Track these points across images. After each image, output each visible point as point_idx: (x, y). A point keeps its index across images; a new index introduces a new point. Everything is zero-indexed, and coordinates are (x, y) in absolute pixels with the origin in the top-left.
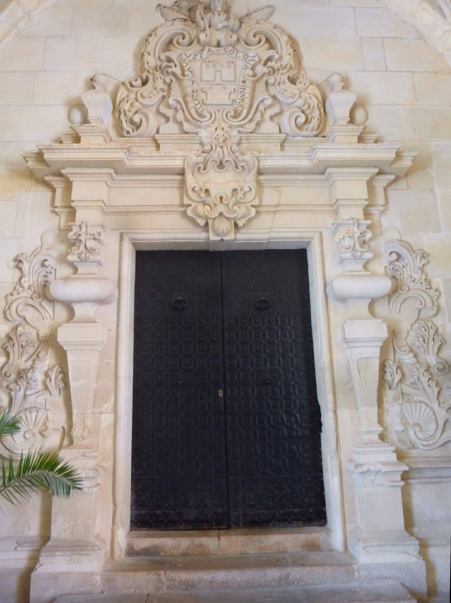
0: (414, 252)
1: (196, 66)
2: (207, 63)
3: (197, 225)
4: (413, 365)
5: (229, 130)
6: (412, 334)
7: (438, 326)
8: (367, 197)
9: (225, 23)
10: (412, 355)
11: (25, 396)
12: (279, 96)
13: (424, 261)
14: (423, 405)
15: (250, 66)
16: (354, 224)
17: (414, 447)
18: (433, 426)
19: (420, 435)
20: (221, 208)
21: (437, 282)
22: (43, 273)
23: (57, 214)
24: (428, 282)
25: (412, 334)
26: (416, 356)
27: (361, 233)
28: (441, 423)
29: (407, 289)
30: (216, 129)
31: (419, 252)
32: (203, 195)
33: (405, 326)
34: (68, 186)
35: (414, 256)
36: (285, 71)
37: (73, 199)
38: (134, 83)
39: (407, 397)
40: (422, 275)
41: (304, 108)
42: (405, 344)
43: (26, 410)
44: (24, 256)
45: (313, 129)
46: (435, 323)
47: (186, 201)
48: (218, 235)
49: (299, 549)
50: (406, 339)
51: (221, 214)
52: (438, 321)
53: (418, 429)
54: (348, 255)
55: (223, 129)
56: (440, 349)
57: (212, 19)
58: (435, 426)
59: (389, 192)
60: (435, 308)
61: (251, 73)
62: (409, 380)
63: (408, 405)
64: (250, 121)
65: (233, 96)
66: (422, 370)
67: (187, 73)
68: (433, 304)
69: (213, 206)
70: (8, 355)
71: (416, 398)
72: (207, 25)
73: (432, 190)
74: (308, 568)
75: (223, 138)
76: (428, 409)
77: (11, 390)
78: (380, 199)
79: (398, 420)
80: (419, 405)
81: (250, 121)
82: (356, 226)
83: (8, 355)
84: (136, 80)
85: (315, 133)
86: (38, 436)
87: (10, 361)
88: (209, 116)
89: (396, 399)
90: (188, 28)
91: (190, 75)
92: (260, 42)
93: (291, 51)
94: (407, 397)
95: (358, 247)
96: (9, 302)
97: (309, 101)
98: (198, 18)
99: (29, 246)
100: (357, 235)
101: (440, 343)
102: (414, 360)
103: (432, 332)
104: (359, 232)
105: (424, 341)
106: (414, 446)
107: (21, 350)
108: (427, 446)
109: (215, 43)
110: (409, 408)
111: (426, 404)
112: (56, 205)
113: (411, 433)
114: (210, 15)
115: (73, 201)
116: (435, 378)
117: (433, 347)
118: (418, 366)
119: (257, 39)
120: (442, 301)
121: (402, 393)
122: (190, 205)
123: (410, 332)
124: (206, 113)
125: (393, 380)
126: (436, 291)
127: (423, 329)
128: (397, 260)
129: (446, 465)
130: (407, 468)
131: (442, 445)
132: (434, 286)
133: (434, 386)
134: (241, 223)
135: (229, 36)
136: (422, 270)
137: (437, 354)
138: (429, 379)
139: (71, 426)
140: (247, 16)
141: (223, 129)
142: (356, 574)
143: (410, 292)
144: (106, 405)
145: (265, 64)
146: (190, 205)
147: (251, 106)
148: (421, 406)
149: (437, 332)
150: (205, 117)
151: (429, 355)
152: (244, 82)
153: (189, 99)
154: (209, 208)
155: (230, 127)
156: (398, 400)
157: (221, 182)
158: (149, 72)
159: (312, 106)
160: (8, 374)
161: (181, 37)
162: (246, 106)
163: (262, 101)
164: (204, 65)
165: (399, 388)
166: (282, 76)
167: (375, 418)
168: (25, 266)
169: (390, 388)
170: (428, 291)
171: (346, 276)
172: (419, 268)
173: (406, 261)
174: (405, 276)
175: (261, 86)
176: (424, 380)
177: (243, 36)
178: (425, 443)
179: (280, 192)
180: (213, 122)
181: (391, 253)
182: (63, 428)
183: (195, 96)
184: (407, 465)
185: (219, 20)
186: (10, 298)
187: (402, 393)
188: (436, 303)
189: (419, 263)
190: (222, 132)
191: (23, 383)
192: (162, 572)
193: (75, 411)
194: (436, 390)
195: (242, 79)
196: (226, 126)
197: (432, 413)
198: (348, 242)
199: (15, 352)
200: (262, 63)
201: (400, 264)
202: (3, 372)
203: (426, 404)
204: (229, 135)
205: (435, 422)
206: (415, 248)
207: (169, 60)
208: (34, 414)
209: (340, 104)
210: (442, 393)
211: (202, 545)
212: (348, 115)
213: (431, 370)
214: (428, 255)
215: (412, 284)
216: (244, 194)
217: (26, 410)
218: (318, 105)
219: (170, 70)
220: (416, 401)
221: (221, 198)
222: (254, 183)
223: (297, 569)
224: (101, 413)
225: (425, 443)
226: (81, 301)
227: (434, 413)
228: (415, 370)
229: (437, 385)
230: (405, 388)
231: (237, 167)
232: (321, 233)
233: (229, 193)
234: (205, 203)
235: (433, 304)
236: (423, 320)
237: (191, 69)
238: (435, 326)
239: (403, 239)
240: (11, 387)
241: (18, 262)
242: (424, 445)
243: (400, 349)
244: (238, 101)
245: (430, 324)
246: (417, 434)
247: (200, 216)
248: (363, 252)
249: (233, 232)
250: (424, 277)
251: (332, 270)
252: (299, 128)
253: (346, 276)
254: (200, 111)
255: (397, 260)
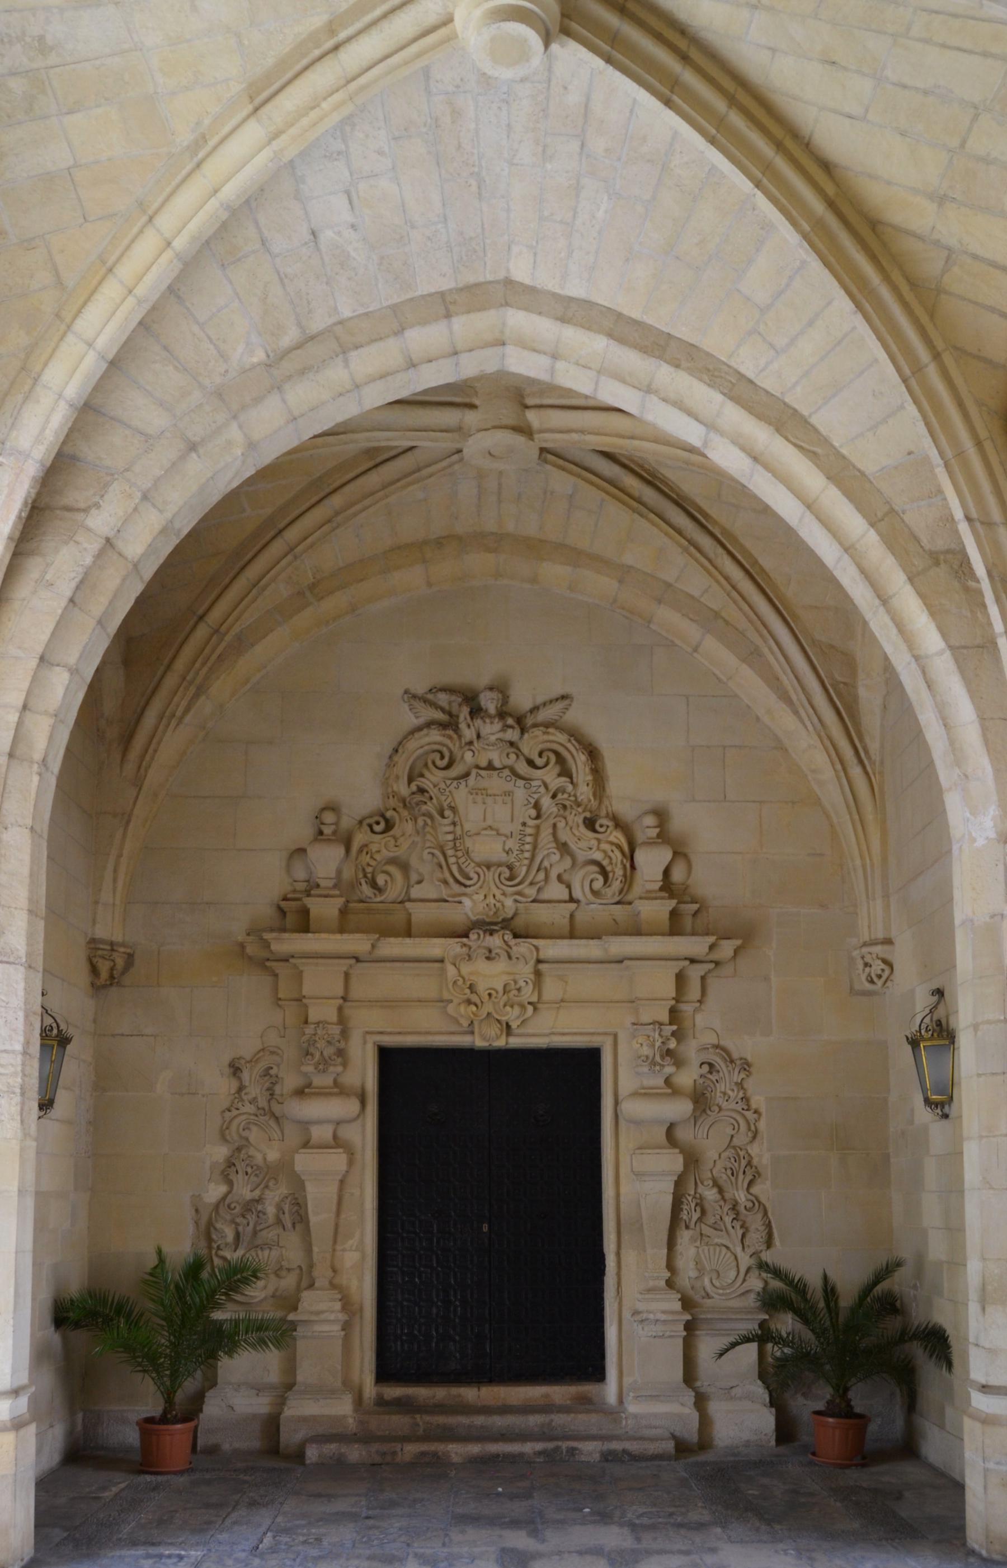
0: (732, 1061)
1: (461, 795)
2: (474, 796)
3: (461, 1025)
4: (716, 1202)
5: (502, 898)
6: (720, 1165)
7: (753, 1155)
8: (674, 995)
9: (500, 735)
10: (715, 1190)
11: (255, 1233)
12: (572, 846)
13: (743, 1075)
14: (724, 1250)
15: (533, 801)
16: (655, 1030)
17: (708, 1296)
18: (733, 1274)
19: (717, 1284)
20: (488, 1007)
21: (758, 1101)
22: (267, 1085)
23: (279, 1006)
24: (746, 1099)
25: (720, 1165)
26: (721, 1191)
27: (663, 1043)
28: (743, 1270)
29: (717, 1109)
30: (485, 896)
31: (738, 1062)
32: (468, 991)
33: (711, 1154)
34: (299, 976)
35: (730, 1068)
36: (580, 810)
37: (304, 993)
38: (377, 828)
39: (706, 1239)
40: (738, 1092)
41: (605, 863)
42: (710, 1175)
43: (257, 1247)
44: (243, 1062)
45: (614, 894)
46: (750, 1151)
47: (446, 996)
48: (484, 1039)
49: (568, 1402)
50: (711, 1170)
51: (489, 1014)
52: (754, 1150)
53: (714, 1276)
54: (646, 1069)
55: (494, 896)
56: (750, 1184)
57: (482, 728)
58: (735, 1273)
59: (709, 981)
60: (750, 1134)
61: (533, 813)
62: (710, 1219)
63: (706, 1248)
64: (531, 884)
65: (510, 844)
66: (726, 1209)
67: (447, 813)
68: (749, 1129)
69: (480, 1004)
70: (230, 1183)
71: (717, 1240)
72: (475, 737)
73: (767, 979)
74: (572, 1415)
75: (494, 910)
76: (729, 1254)
77: (237, 1224)
78: (694, 991)
79: (692, 1265)
80: (718, 1249)
81: (531, 884)
82: (657, 1033)
83: (230, 1183)
84: (378, 823)
85: (617, 899)
86: (272, 1276)
87: (234, 1191)
88: (476, 877)
89: (693, 1240)
90: (448, 742)
91: (452, 815)
92: (547, 764)
93: (590, 778)
94: (706, 1239)
95: (658, 1059)
96: (228, 1119)
97: (611, 854)
98: (463, 726)
99: (247, 1047)
100: (658, 1044)
101: (751, 1177)
102: (718, 1197)
103: (744, 1163)
104: (660, 1040)
105: (733, 1174)
106: (708, 1295)
107: (246, 1178)
108: (722, 1295)
109: (484, 763)
110: (706, 1251)
111: (727, 1248)
112: (280, 996)
113: (706, 1281)
114: (478, 722)
115: (304, 997)
116: (742, 1217)
117: (743, 1181)
118: (722, 1203)
119: (544, 760)
120: (762, 1125)
121: (701, 1234)
122: (451, 1001)
123: (718, 1162)
124: (472, 875)
125: (690, 1220)
126: (756, 1112)
127: (733, 1160)
128: (710, 1072)
129: (739, 1316)
130: (689, 1317)
131: (743, 1294)
132: (754, 1106)
133: (738, 1227)
134: (514, 1025)
135: (505, 755)
136: (740, 1085)
137: (748, 1189)
138: (734, 1219)
139: (311, 1266)
140: (531, 711)
141: (494, 896)
142: (624, 1422)
143: (722, 1113)
144: (350, 1242)
145: (554, 796)
146: (451, 1001)
147: (532, 859)
148: (720, 1251)
149: (749, 1164)
150: (471, 879)
151: (737, 1190)
152: (524, 824)
153: (450, 852)
154: (474, 1008)
155: (504, 894)
156: (695, 1241)
157: (491, 975)
158: (394, 809)
159: (614, 861)
160: (233, 1206)
161: (438, 756)
162: (526, 862)
163: (548, 855)
164: (471, 797)
165: (698, 1228)
166: (576, 819)
167: (664, 1263)
168: (246, 1075)
169: (687, 1227)
170: (744, 1112)
171: (641, 1094)
172: (736, 1083)
173: (721, 1074)
174: (718, 1094)
175: (546, 833)
176: (728, 1220)
177: (526, 750)
178: (721, 1291)
179: (566, 982)
180: (481, 887)
181: (702, 1064)
182: (300, 1267)
183: (458, 845)
184: (692, 1315)
185: (491, 729)
186: (227, 1114)
187: (701, 1234)
188: (753, 1128)
189: (737, 1077)
190: (493, 901)
191: (252, 1218)
192: (418, 1416)
193: (315, 1249)
194: (740, 1232)
195: (521, 820)
196: (498, 893)
197: (733, 1257)
198: (646, 1051)
199: (239, 1180)
200: (551, 794)
201: (713, 1077)
202: (226, 1203)
203: (727, 1248)
204: (503, 906)
205: (735, 1269)
206: (735, 1055)
207: (422, 791)
208: (266, 1252)
209: (651, 862)
210: (748, 1236)
211: (460, 1396)
212: (660, 877)
213: (737, 1208)
214: (749, 1065)
215: (726, 1103)
216: (519, 990)
217: (257, 1247)
218: (622, 861)
219: (424, 807)
220: (717, 1244)
221: (490, 995)
222: (532, 976)
223: (561, 1415)
224: (344, 1250)
225: (721, 1291)
226: (319, 1122)
227: (736, 1258)
228: (718, 1208)
229: (742, 1227)
230: (706, 1230)
231: (510, 957)
232: (615, 1036)
233: (500, 989)
234: (469, 1002)
235: (749, 1129)
236: (734, 1148)
237: (453, 804)
238: (749, 1155)
239: (722, 1043)
240: (238, 1220)
241: (235, 1069)
242: (720, 1295)
243: (702, 1184)
244: (516, 853)
245: (742, 1153)
246: (714, 1281)
247: (462, 1016)
248: (663, 1066)
249: (504, 1036)
250: (741, 1095)
251: (627, 1083)
252: (595, 893)
253: (641, 1094)
254: (463, 866)
255: (710, 1072)
